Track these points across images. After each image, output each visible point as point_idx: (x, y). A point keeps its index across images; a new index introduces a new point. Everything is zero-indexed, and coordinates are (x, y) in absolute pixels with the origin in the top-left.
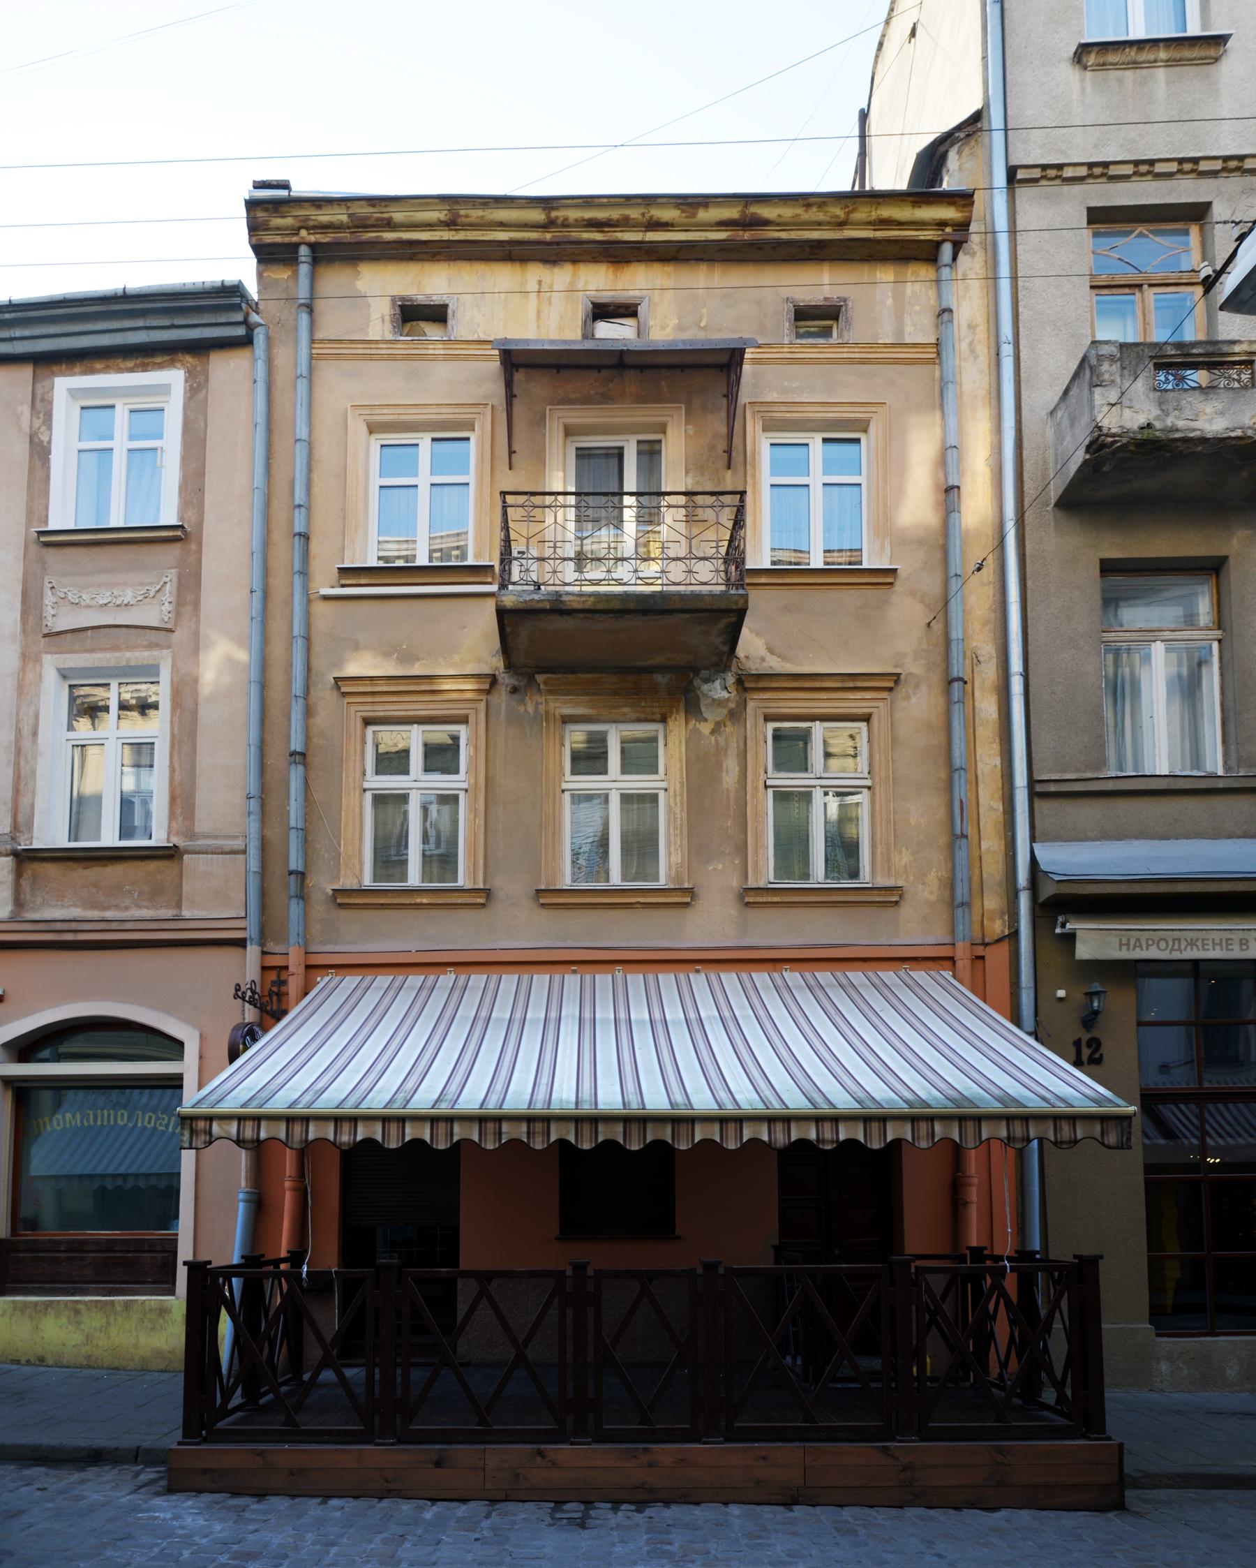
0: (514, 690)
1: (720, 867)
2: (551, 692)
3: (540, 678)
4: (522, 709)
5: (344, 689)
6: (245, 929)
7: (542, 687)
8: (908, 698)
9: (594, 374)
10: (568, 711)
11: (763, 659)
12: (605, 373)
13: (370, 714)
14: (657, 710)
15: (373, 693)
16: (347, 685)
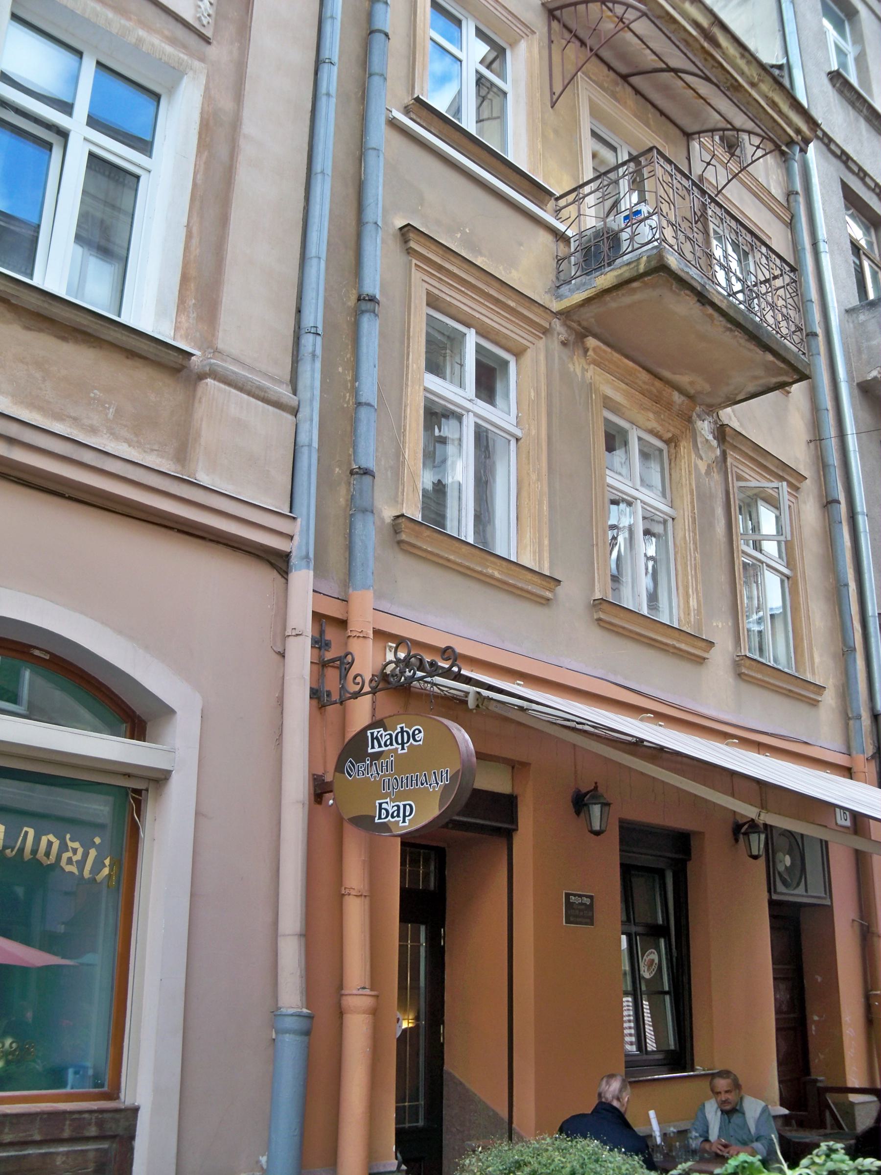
0: (564, 344)
1: (720, 626)
2: (595, 363)
3: (591, 342)
4: (571, 366)
5: (412, 244)
6: (291, 537)
7: (590, 353)
8: (805, 503)
9: (605, 69)
10: (610, 392)
11: (730, 418)
12: (611, 73)
13: (436, 292)
14: (672, 429)
15: (440, 268)
16: (418, 242)
